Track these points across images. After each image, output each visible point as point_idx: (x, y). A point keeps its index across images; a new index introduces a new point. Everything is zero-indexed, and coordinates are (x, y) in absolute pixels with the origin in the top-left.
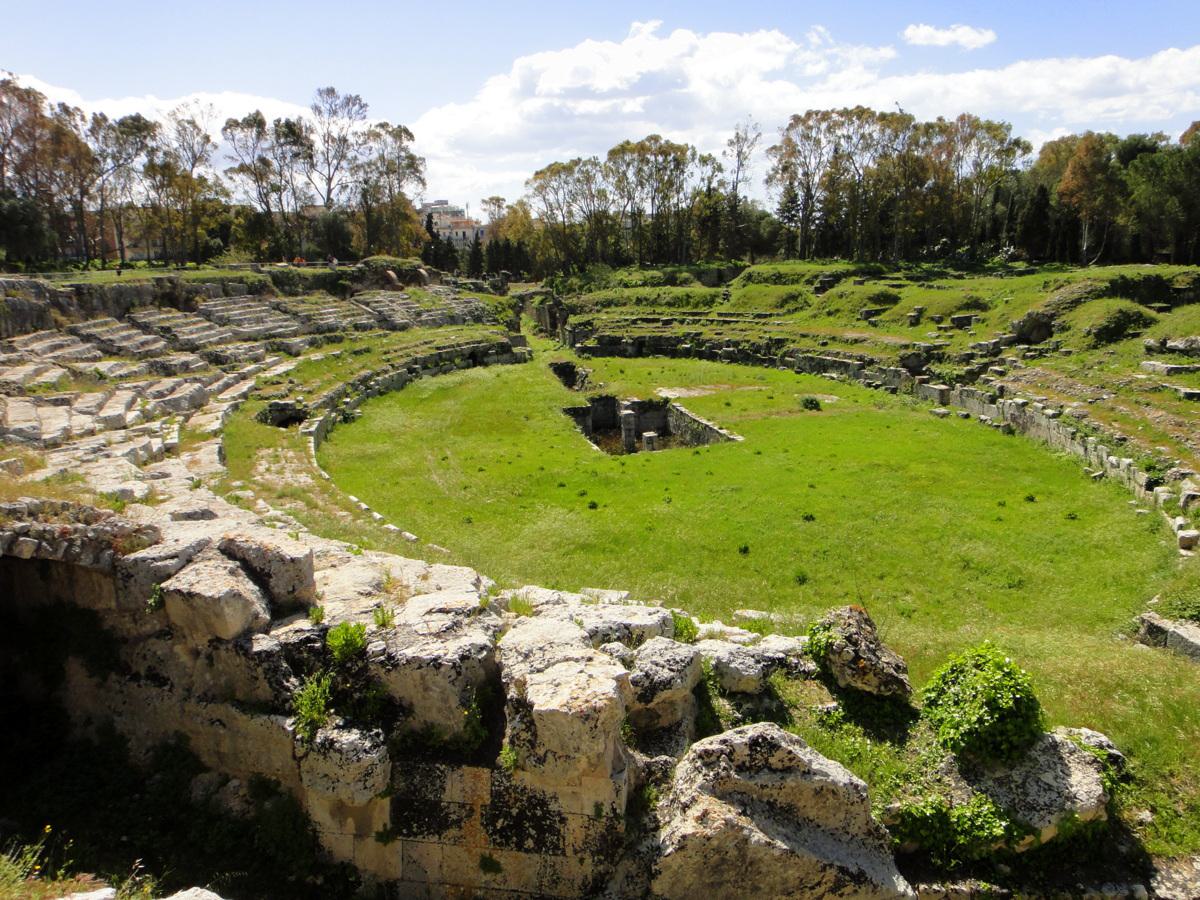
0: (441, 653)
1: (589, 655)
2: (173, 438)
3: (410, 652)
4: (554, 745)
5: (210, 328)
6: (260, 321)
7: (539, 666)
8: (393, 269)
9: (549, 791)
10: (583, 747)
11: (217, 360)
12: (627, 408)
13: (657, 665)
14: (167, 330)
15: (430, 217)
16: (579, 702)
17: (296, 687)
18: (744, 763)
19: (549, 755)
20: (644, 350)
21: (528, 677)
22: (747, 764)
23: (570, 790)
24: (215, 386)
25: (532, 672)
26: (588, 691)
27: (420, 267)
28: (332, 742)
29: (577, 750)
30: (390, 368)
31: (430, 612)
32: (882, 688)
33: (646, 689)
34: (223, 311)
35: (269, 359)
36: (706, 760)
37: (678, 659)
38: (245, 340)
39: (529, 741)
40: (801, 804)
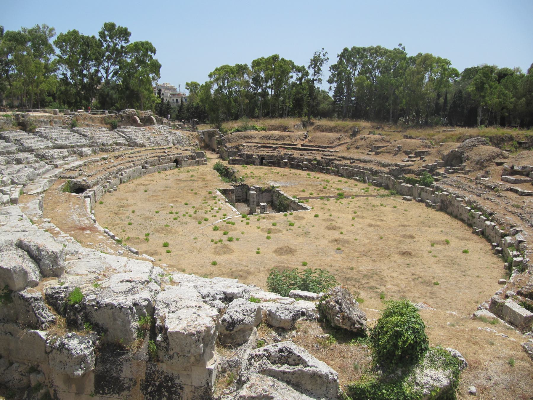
0: (123, 301)
1: (199, 305)
2: (16, 195)
3: (107, 301)
4: (178, 350)
5: (42, 141)
6: (67, 139)
7: (173, 310)
9: (175, 374)
10: (192, 351)
11: (42, 157)
12: (253, 190)
13: (237, 312)
14: (18, 141)
15: (160, 91)
16: (190, 328)
17: (49, 317)
19: (175, 355)
20: (264, 161)
21: (167, 315)
23: (185, 373)
24: (41, 171)
25: (169, 313)
26: (196, 323)
27: (151, 115)
28: (64, 345)
29: (189, 352)
31: (122, 282)
32: (352, 327)
34: (48, 133)
35: (70, 158)
37: (248, 309)
38: (59, 148)
39: (166, 348)
40: (303, 382)
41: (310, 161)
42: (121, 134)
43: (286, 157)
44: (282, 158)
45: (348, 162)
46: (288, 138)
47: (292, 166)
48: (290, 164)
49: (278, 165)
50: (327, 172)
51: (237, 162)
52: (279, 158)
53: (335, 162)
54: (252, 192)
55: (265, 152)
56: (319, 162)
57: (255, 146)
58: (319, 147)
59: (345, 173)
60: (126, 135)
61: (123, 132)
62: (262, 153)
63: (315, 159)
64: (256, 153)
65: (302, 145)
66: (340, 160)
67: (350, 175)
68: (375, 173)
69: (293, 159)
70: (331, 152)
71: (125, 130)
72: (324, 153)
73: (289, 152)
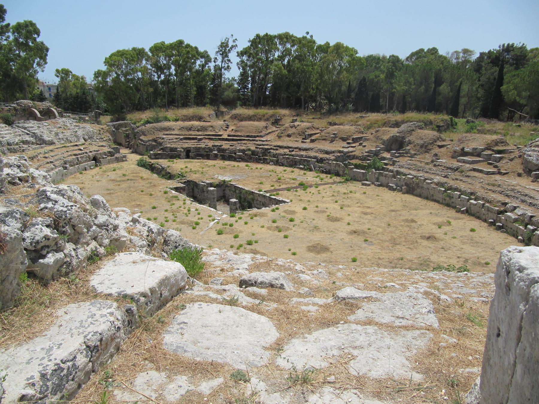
41: (243, 151)
42: (23, 130)
43: (216, 148)
44: (211, 150)
45: (286, 150)
46: (211, 128)
47: (224, 158)
48: (221, 155)
49: (208, 157)
50: (265, 162)
51: (160, 157)
52: (207, 150)
53: (272, 151)
55: (190, 144)
56: (253, 153)
57: (176, 139)
58: (248, 136)
59: (285, 162)
60: (29, 131)
61: (25, 128)
62: (186, 146)
63: (249, 150)
64: (180, 146)
65: (229, 136)
66: (277, 150)
67: (293, 164)
68: (321, 161)
69: (224, 150)
70: (263, 141)
71: (26, 125)
72: (257, 143)
73: (218, 143)
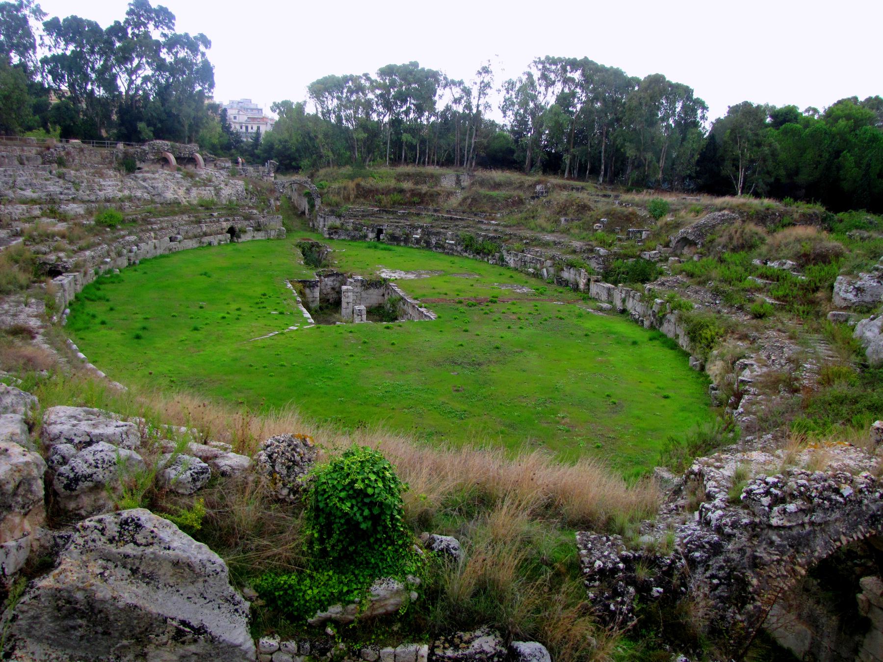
8: (173, 153)
18: (114, 538)
22: (117, 538)
30: (153, 234)
33: (71, 480)
36: (82, 532)
54: (344, 288)
